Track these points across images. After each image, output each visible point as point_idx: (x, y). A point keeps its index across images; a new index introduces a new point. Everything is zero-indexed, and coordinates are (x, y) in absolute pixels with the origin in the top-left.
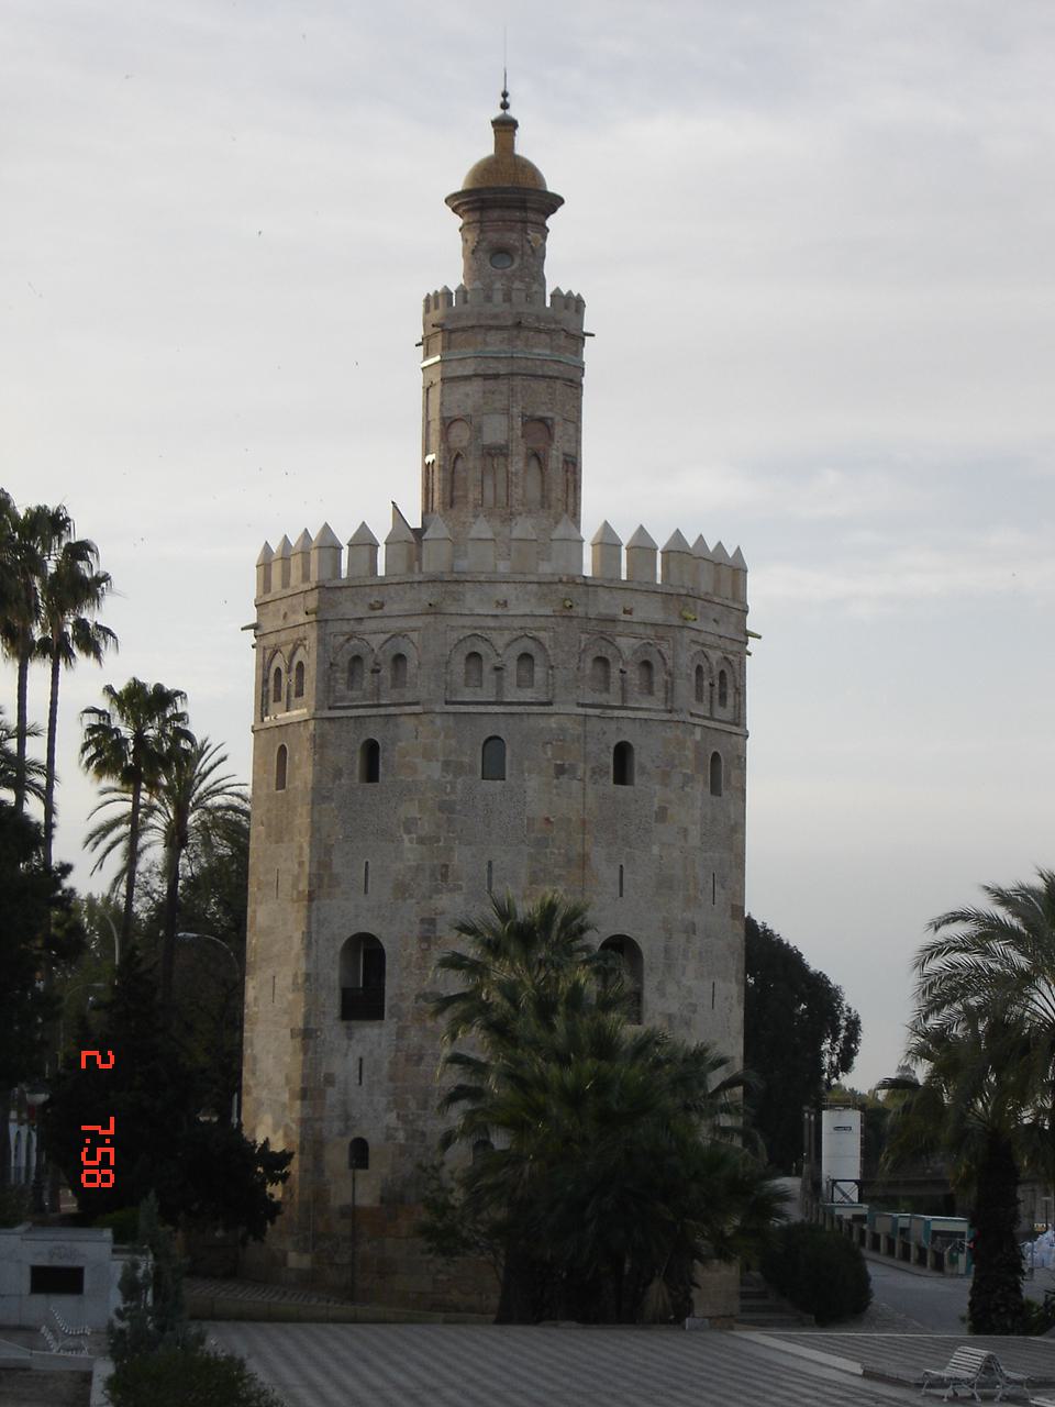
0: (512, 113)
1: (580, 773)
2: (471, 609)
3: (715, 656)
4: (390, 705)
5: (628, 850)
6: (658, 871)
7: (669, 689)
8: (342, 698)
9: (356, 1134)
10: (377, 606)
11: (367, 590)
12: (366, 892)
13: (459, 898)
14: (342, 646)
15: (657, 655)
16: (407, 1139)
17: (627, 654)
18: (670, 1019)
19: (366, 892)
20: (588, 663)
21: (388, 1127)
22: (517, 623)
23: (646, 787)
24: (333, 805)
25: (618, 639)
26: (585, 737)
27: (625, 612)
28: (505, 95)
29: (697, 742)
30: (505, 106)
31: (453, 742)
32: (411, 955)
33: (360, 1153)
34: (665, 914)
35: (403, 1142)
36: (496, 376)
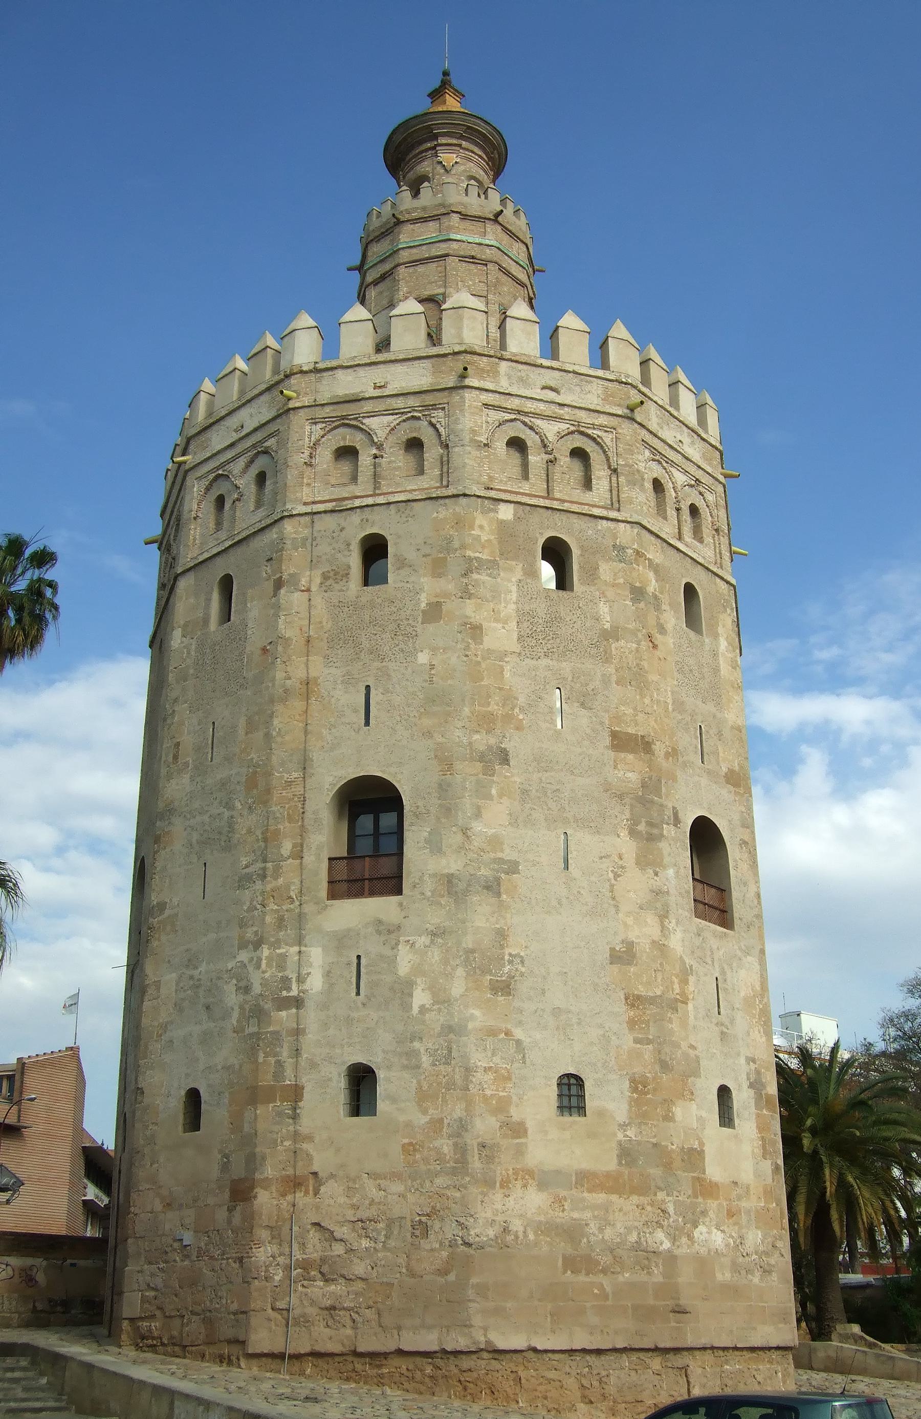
1: (304, 581)
3: (551, 430)
5: (377, 664)
6: (426, 685)
7: (445, 463)
13: (186, 779)
15: (431, 430)
17: (380, 435)
18: (449, 882)
20: (325, 455)
22: (248, 443)
23: (411, 580)
25: (365, 421)
26: (314, 539)
27: (376, 387)
29: (502, 523)
31: (192, 600)
34: (441, 740)
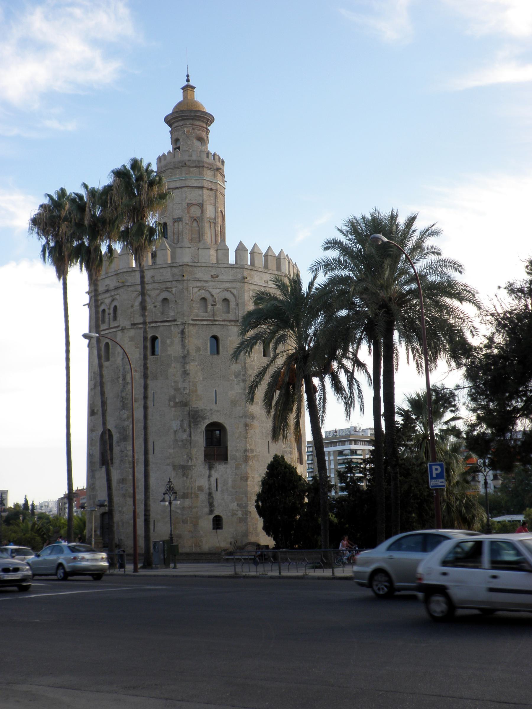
0: (191, 83)
2: (257, 282)
4: (224, 321)
8: (197, 316)
9: (216, 513)
10: (215, 276)
11: (210, 269)
12: (216, 403)
14: (197, 292)
16: (243, 515)
19: (216, 403)
21: (233, 510)
24: (196, 363)
28: (188, 76)
30: (188, 81)
32: (241, 432)
33: (218, 522)
35: (241, 516)
36: (211, 189)
